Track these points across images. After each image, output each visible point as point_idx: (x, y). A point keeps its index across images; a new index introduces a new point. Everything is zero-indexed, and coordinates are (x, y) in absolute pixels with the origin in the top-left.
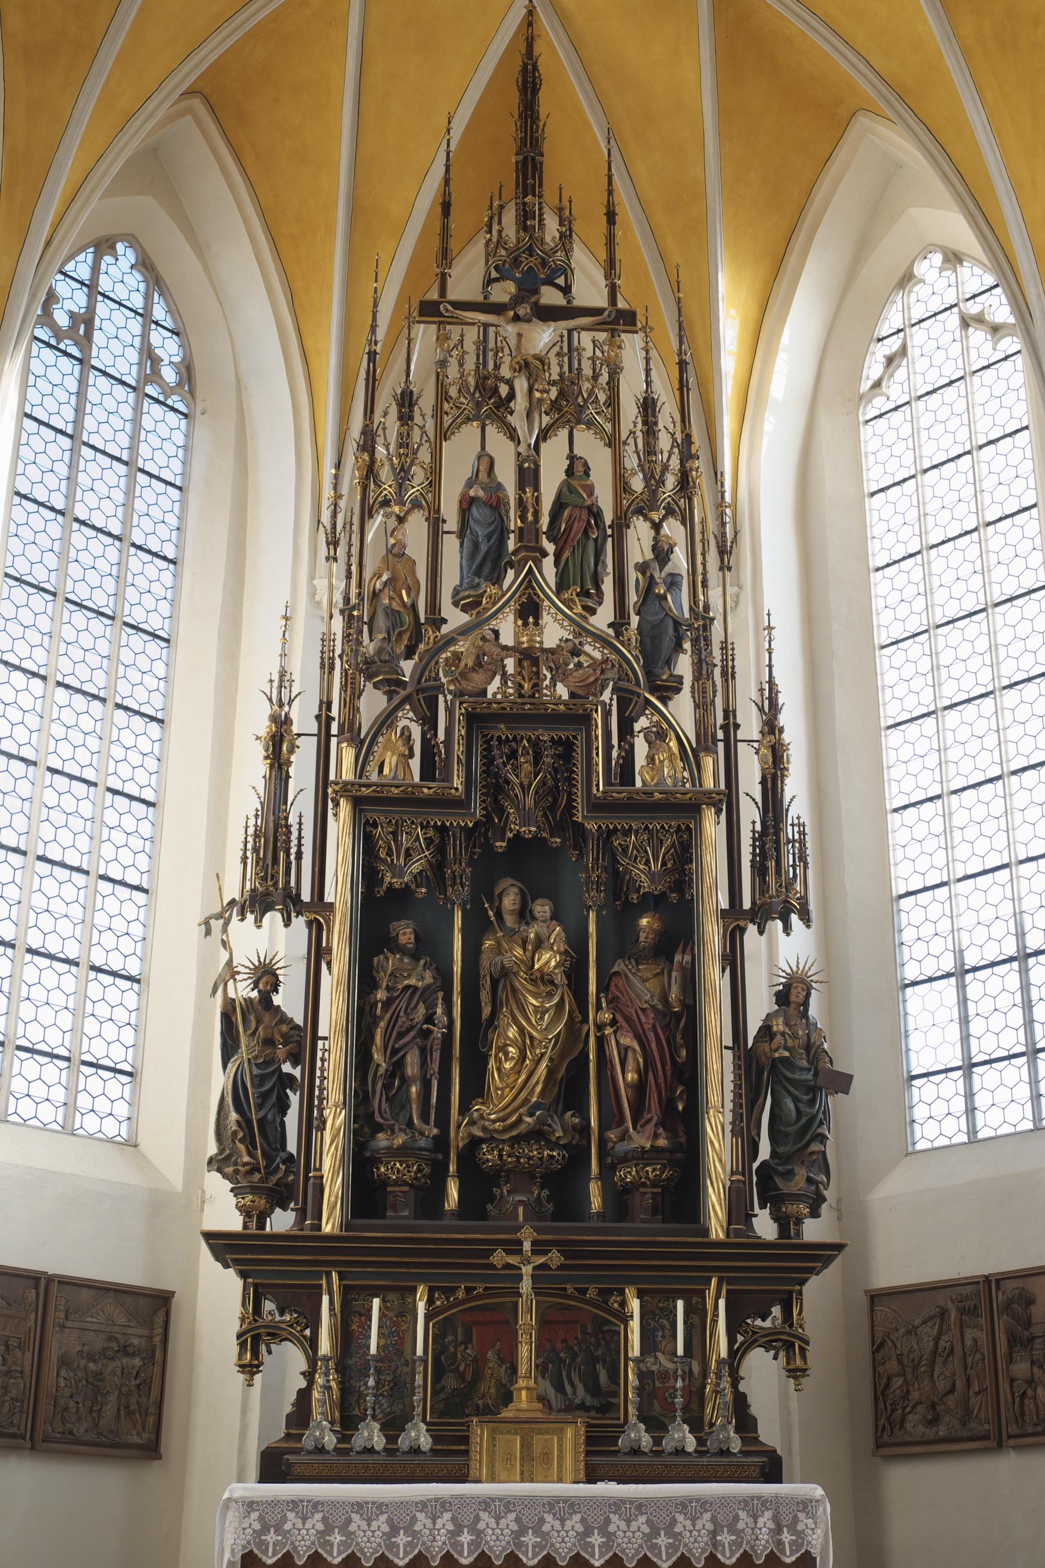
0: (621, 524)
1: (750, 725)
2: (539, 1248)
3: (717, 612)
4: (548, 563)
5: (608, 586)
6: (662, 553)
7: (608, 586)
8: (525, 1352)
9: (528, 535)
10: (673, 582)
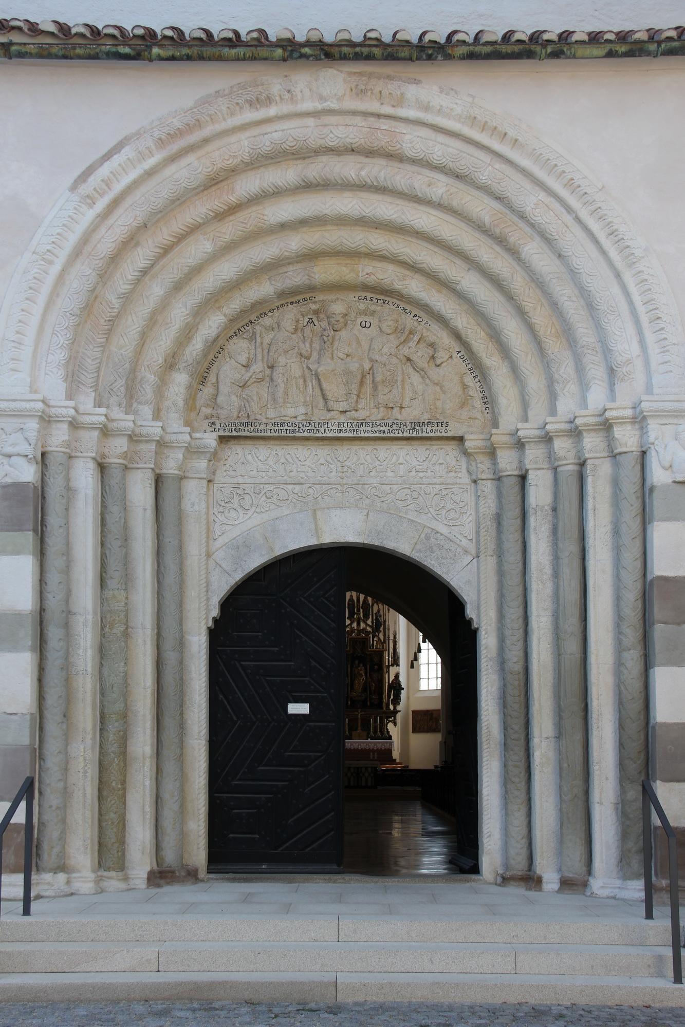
0: (373, 605)
1: (392, 637)
2: (361, 712)
3: (387, 620)
4: (362, 614)
5: (371, 616)
6: (379, 611)
7: (371, 616)
8: (359, 724)
9: (359, 610)
10: (380, 616)
